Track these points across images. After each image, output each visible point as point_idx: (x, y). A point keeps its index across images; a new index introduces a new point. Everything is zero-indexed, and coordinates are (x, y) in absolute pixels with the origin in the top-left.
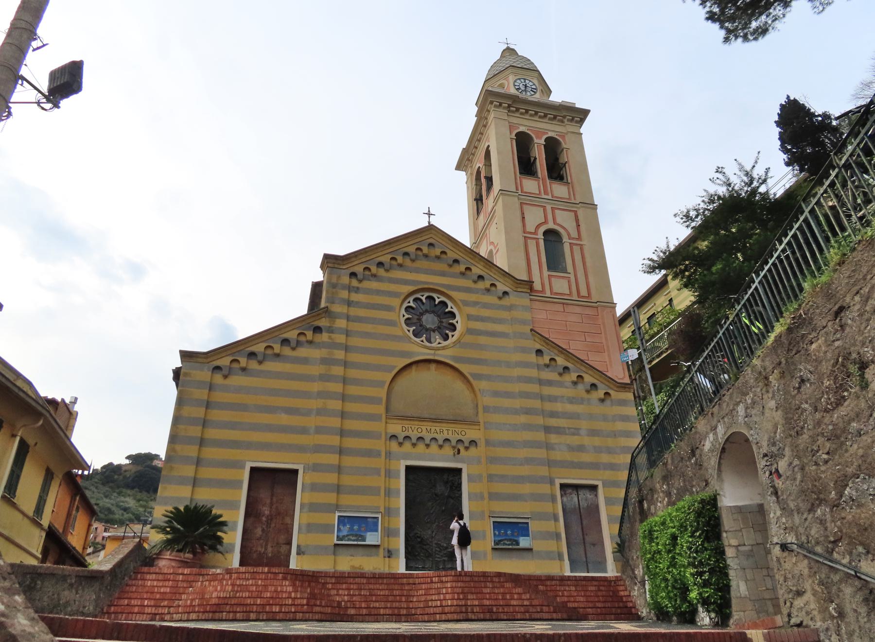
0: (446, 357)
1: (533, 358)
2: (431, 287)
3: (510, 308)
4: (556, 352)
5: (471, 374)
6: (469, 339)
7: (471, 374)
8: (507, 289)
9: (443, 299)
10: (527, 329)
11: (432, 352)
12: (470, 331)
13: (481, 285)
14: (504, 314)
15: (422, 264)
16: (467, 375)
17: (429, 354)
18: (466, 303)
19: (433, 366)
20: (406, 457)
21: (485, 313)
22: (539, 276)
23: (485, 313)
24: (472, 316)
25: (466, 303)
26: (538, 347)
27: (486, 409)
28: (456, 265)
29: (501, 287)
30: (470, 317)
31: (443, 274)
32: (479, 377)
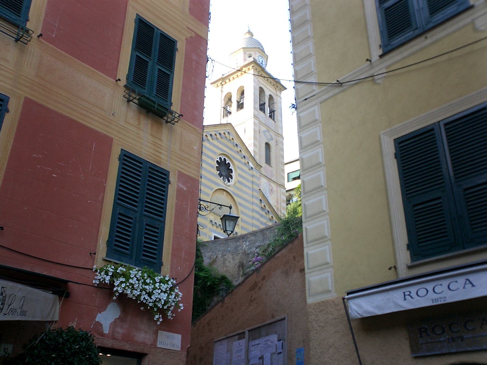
0: (230, 191)
1: (258, 202)
2: (227, 154)
3: (253, 176)
5: (238, 202)
8: (253, 167)
9: (229, 162)
10: (257, 188)
11: (226, 186)
15: (224, 141)
16: (237, 202)
17: (225, 187)
18: (239, 168)
19: (225, 193)
20: (215, 232)
22: (263, 163)
30: (239, 175)
32: (241, 204)
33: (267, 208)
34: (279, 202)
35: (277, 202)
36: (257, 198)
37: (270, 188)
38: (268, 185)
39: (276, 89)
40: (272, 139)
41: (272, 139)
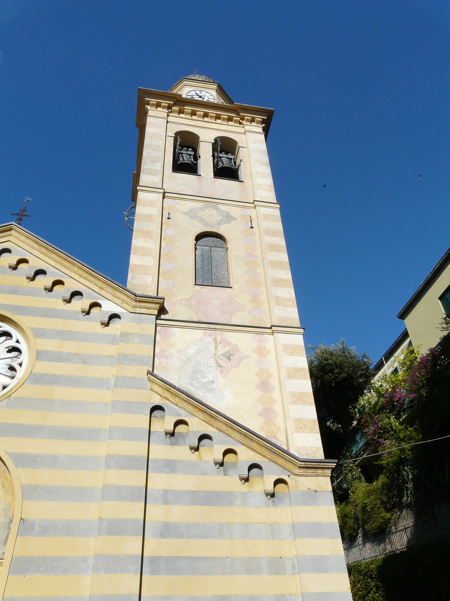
3: (125, 337)
4: (190, 408)
6: (30, 391)
7: (10, 455)
12: (34, 378)
13: (79, 304)
14: (111, 350)
18: (40, 333)
21: (70, 347)
23: (70, 347)
24: (47, 353)
25: (40, 333)
26: (157, 401)
27: (26, 527)
28: (39, 277)
29: (109, 307)
31: (14, 291)
32: (26, 461)
33: (197, 425)
34: (274, 381)
35: (264, 386)
36: (127, 407)
37: (222, 350)
38: (213, 345)
39: (240, 123)
40: (229, 218)
41: (229, 218)
